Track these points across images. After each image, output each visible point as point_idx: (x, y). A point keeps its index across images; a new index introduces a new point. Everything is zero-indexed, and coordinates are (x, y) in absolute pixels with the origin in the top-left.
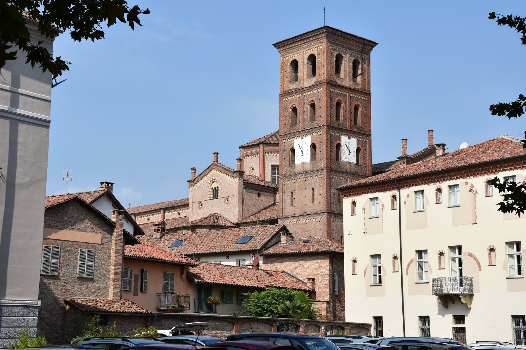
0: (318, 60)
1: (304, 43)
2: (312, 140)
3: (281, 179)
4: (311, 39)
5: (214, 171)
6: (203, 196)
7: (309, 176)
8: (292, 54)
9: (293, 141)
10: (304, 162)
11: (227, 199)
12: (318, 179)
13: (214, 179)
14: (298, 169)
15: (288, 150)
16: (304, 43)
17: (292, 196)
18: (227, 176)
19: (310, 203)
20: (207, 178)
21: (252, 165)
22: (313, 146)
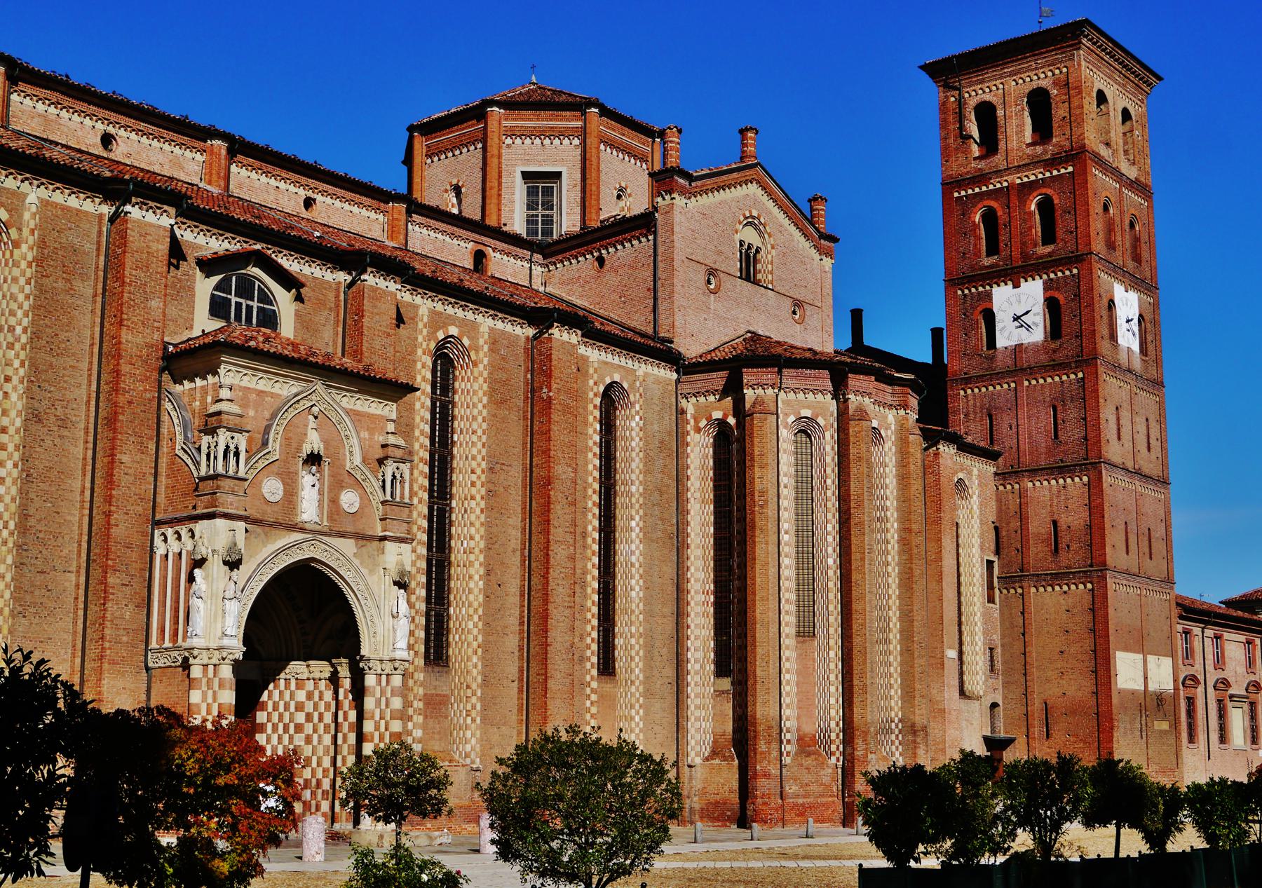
1: (1121, 72)
4: (1132, 77)
5: (753, 189)
6: (720, 253)
13: (754, 217)
15: (1105, 302)
16: (1121, 72)
17: (1118, 419)
18: (797, 234)
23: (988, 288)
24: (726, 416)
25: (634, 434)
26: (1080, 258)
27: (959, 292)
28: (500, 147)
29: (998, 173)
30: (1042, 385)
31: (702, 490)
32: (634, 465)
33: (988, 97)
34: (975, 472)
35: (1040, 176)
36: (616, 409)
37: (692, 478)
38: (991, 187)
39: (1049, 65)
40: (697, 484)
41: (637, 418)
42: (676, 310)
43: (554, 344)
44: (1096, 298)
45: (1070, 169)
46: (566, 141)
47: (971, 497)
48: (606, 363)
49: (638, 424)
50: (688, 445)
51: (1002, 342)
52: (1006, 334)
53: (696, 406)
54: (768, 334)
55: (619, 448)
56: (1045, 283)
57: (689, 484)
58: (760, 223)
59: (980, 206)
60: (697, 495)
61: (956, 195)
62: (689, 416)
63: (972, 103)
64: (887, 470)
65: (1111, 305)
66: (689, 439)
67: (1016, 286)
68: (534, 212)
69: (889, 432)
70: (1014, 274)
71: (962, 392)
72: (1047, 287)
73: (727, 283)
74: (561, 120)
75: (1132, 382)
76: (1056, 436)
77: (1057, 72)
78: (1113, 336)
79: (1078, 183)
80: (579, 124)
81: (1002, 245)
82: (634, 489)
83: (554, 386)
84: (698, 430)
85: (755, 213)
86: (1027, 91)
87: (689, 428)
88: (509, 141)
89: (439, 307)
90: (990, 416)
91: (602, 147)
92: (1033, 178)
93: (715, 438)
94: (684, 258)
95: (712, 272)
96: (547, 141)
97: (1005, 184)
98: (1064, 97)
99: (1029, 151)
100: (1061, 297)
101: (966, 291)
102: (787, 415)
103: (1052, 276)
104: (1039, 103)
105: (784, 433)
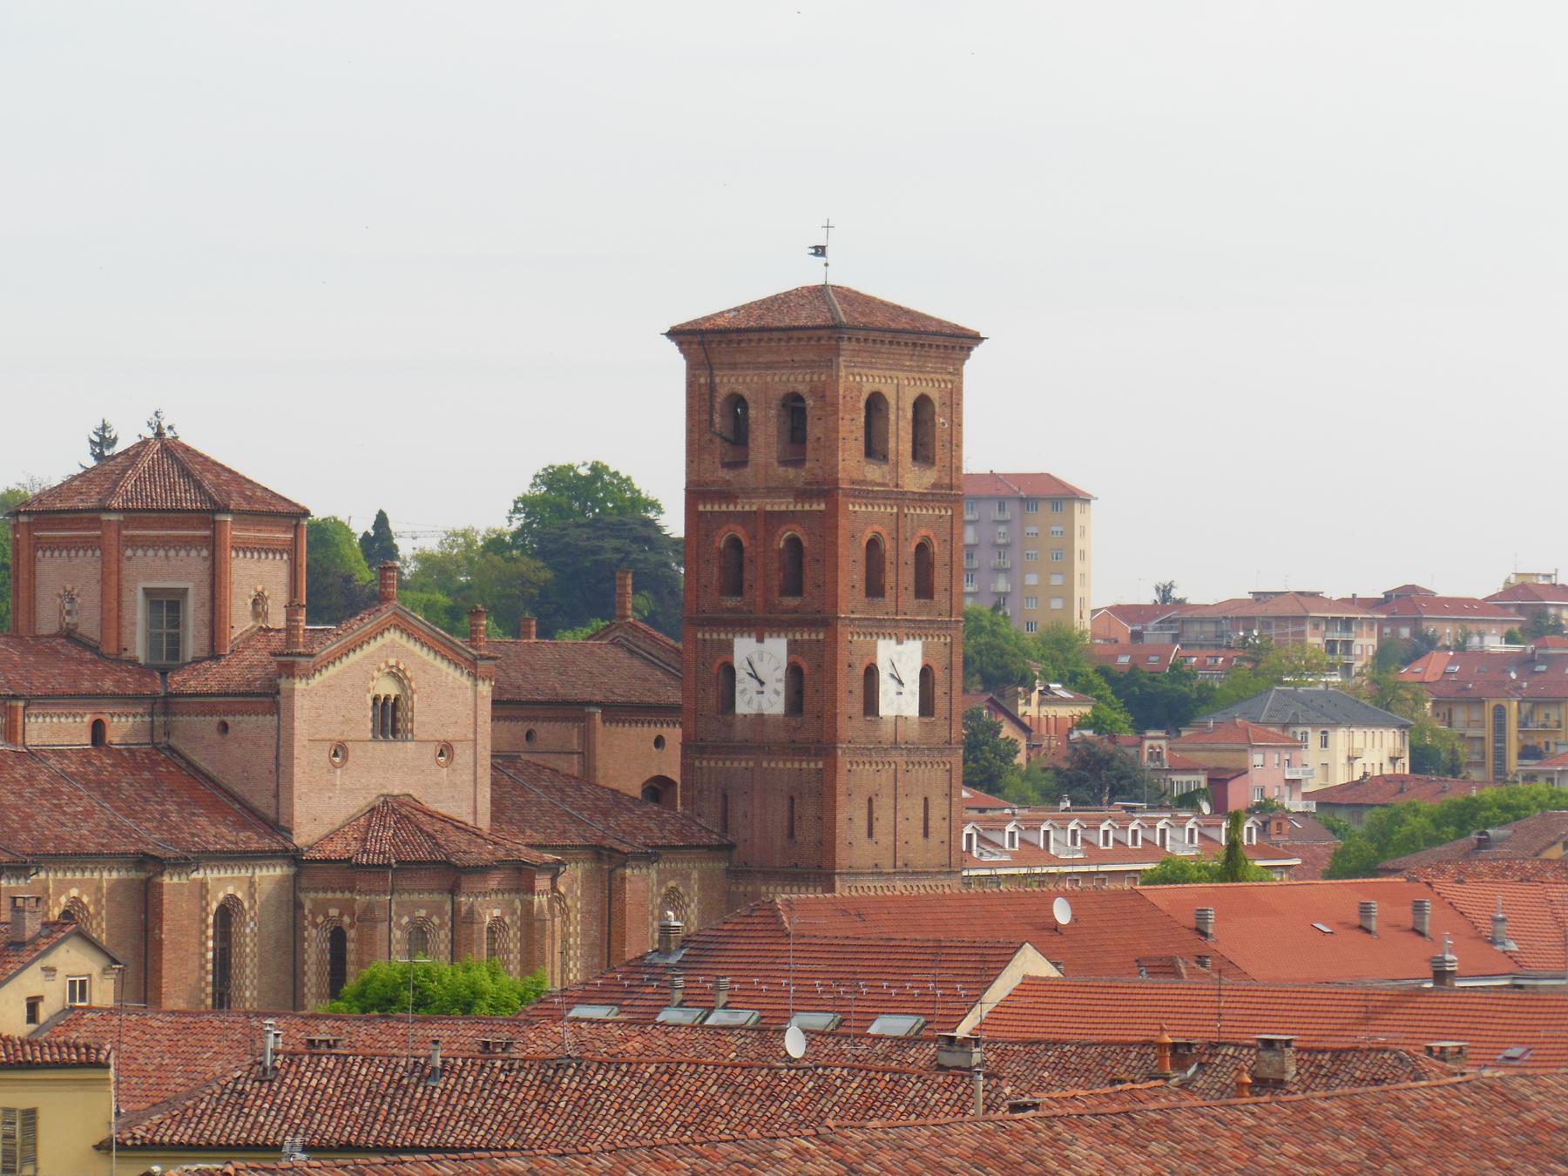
0: (942, 420)
2: (925, 654)
3: (844, 753)
6: (347, 721)
7: (917, 759)
8: (875, 372)
9: (875, 643)
10: (904, 714)
11: (446, 750)
12: (939, 773)
14: (886, 732)
15: (860, 671)
18: (443, 665)
19: (917, 838)
20: (365, 657)
21: (260, 588)
22: (926, 674)
23: (730, 636)
24: (341, 915)
25: (248, 940)
26: (826, 621)
27: (700, 635)
28: (119, 561)
29: (749, 494)
30: (781, 770)
31: (318, 985)
32: (248, 971)
33: (740, 389)
34: (695, 875)
35: (791, 508)
36: (231, 916)
37: (309, 974)
38: (739, 508)
39: (807, 367)
40: (314, 979)
41: (252, 924)
42: (296, 800)
43: (165, 890)
44: (842, 668)
45: (822, 507)
46: (193, 553)
47: (688, 906)
48: (219, 879)
49: (252, 930)
50: (305, 940)
51: (742, 707)
52: (747, 698)
53: (314, 901)
54: (406, 791)
55: (234, 955)
56: (789, 644)
57: (306, 979)
58: (399, 670)
59: (725, 529)
60: (314, 990)
61: (701, 508)
62: (306, 912)
63: (722, 392)
64: (511, 956)
65: (871, 673)
66: (306, 934)
67: (760, 640)
68: (158, 631)
69: (515, 918)
70: (760, 627)
71: (697, 763)
72: (793, 647)
73: (355, 751)
74: (188, 529)
75: (897, 759)
76: (791, 835)
77: (815, 377)
78: (871, 704)
79: (827, 524)
80: (207, 533)
81: (746, 585)
82: (248, 994)
83: (165, 928)
84: (315, 925)
85: (392, 662)
86: (782, 393)
87: (306, 923)
88: (129, 552)
89: (60, 875)
90: (725, 797)
91: (234, 554)
92: (783, 508)
93: (332, 932)
94: (306, 742)
95: (340, 750)
96: (172, 553)
97: (754, 508)
98: (819, 412)
99: (781, 470)
100: (805, 666)
101: (707, 636)
102: (400, 916)
103: (798, 637)
104: (794, 407)
105: (397, 934)
